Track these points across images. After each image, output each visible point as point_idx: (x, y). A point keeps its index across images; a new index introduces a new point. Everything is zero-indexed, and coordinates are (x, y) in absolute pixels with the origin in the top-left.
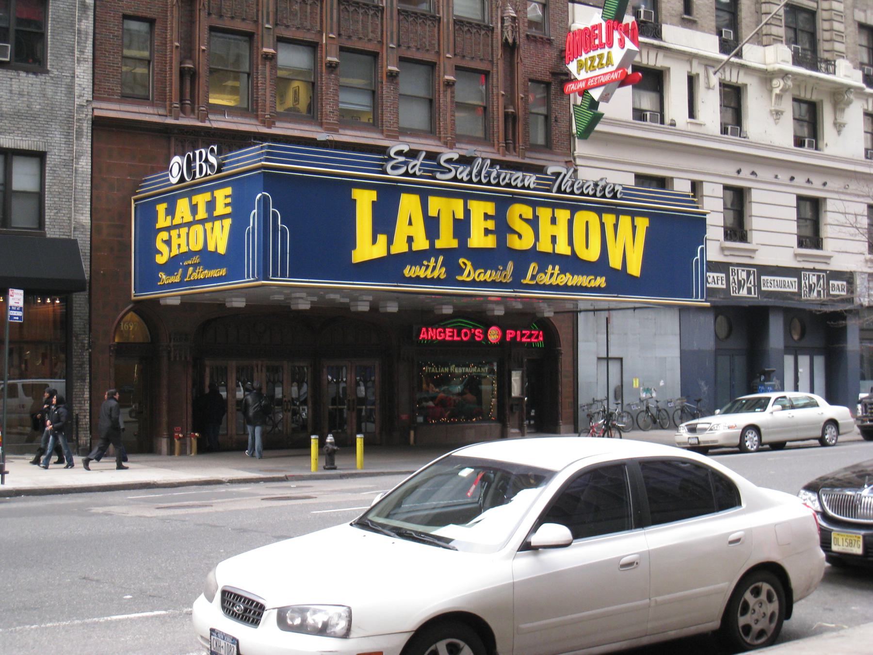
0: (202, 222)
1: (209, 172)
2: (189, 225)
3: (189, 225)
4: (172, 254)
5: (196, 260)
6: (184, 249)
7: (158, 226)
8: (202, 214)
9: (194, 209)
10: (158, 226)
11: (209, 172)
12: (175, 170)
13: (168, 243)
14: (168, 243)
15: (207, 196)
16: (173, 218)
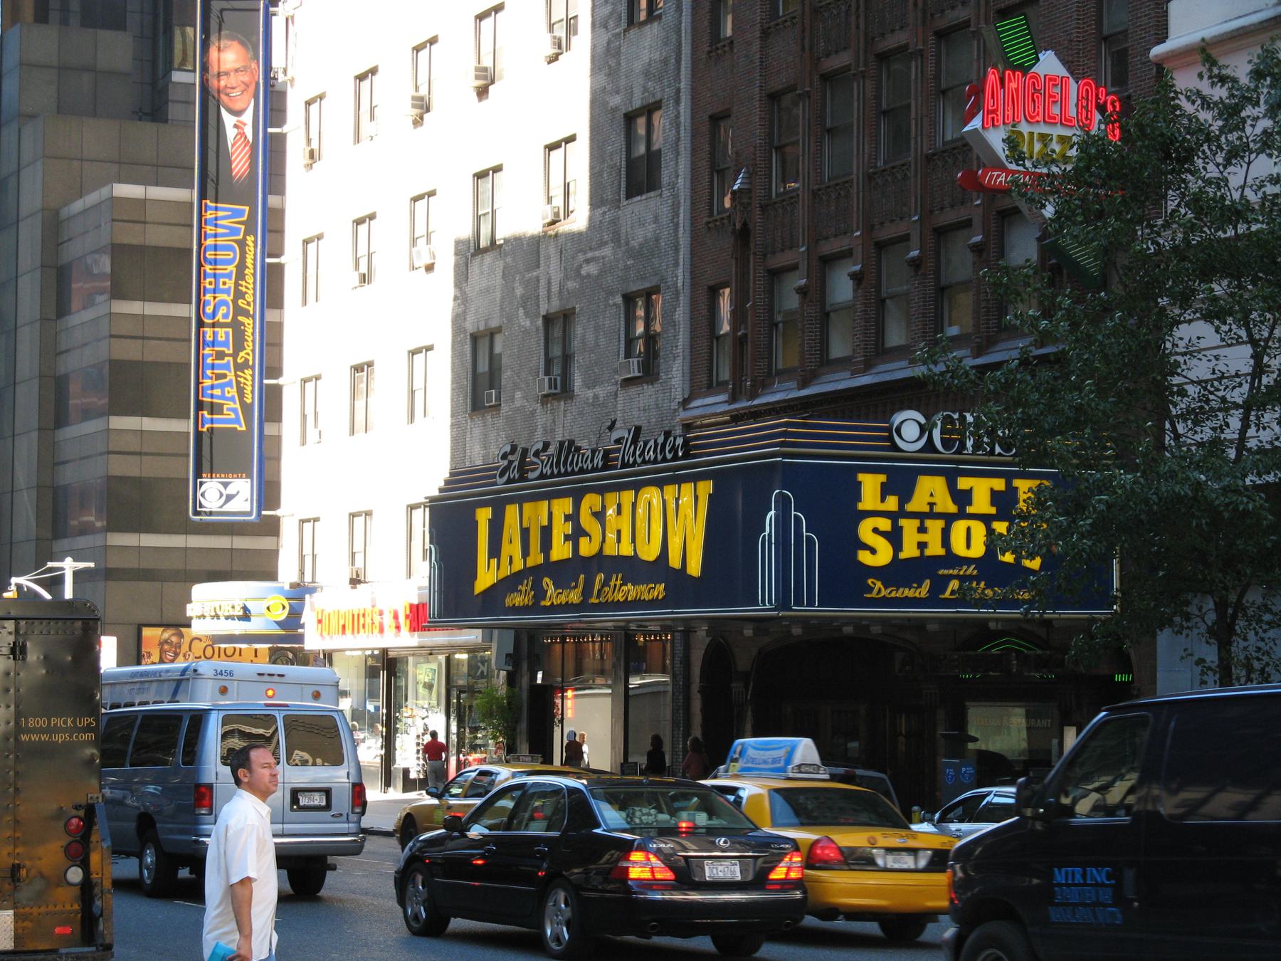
0: (986, 519)
1: (998, 449)
2: (949, 519)
3: (949, 519)
4: (902, 555)
5: (971, 570)
6: (935, 549)
7: (861, 506)
8: (981, 503)
9: (963, 498)
10: (861, 506)
11: (998, 449)
12: (910, 431)
13: (894, 537)
14: (894, 537)
15: (999, 484)
16: (905, 497)
